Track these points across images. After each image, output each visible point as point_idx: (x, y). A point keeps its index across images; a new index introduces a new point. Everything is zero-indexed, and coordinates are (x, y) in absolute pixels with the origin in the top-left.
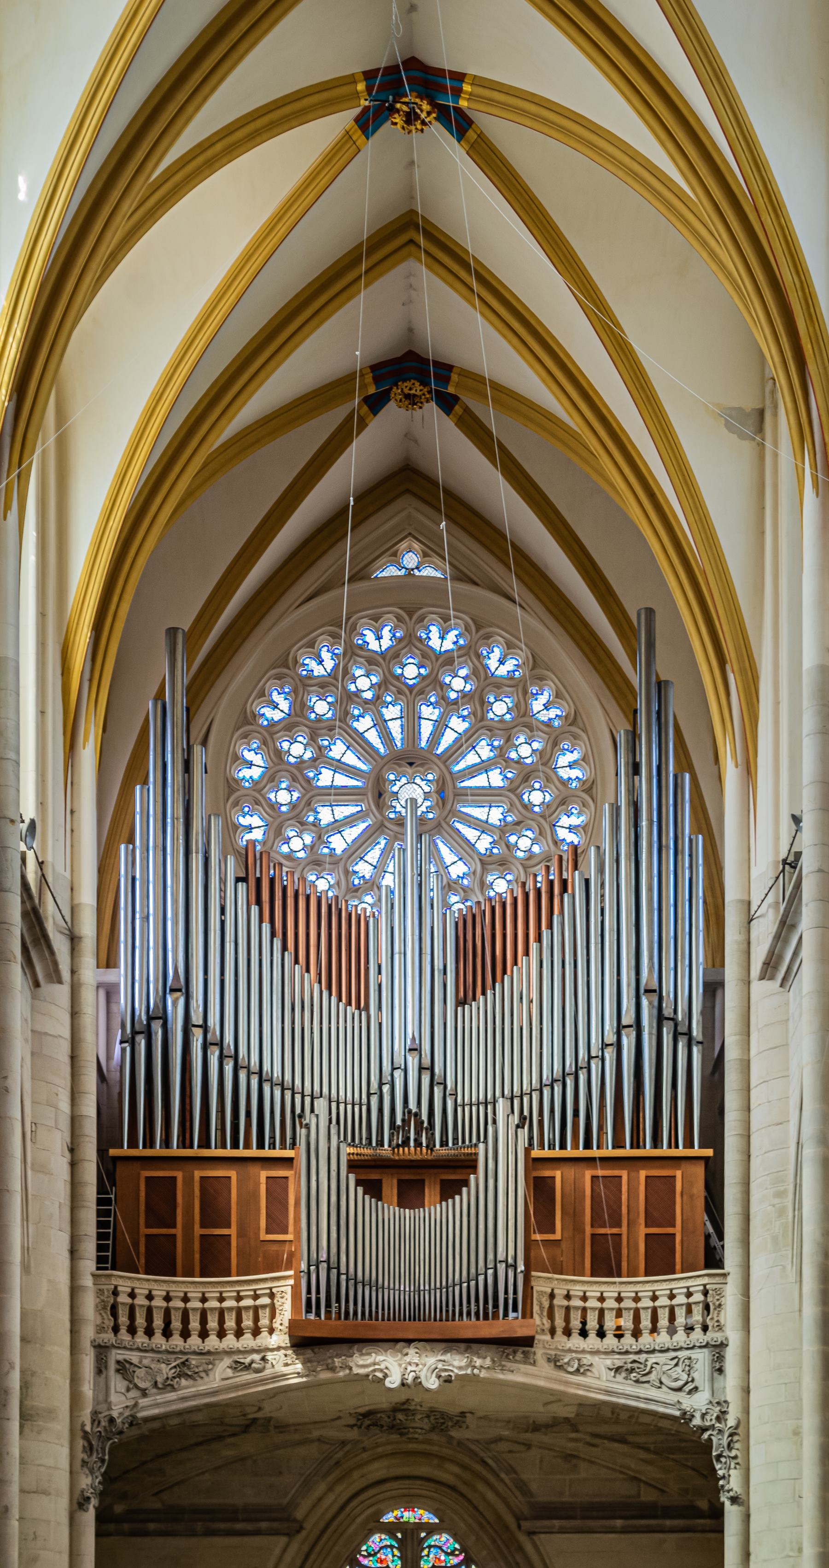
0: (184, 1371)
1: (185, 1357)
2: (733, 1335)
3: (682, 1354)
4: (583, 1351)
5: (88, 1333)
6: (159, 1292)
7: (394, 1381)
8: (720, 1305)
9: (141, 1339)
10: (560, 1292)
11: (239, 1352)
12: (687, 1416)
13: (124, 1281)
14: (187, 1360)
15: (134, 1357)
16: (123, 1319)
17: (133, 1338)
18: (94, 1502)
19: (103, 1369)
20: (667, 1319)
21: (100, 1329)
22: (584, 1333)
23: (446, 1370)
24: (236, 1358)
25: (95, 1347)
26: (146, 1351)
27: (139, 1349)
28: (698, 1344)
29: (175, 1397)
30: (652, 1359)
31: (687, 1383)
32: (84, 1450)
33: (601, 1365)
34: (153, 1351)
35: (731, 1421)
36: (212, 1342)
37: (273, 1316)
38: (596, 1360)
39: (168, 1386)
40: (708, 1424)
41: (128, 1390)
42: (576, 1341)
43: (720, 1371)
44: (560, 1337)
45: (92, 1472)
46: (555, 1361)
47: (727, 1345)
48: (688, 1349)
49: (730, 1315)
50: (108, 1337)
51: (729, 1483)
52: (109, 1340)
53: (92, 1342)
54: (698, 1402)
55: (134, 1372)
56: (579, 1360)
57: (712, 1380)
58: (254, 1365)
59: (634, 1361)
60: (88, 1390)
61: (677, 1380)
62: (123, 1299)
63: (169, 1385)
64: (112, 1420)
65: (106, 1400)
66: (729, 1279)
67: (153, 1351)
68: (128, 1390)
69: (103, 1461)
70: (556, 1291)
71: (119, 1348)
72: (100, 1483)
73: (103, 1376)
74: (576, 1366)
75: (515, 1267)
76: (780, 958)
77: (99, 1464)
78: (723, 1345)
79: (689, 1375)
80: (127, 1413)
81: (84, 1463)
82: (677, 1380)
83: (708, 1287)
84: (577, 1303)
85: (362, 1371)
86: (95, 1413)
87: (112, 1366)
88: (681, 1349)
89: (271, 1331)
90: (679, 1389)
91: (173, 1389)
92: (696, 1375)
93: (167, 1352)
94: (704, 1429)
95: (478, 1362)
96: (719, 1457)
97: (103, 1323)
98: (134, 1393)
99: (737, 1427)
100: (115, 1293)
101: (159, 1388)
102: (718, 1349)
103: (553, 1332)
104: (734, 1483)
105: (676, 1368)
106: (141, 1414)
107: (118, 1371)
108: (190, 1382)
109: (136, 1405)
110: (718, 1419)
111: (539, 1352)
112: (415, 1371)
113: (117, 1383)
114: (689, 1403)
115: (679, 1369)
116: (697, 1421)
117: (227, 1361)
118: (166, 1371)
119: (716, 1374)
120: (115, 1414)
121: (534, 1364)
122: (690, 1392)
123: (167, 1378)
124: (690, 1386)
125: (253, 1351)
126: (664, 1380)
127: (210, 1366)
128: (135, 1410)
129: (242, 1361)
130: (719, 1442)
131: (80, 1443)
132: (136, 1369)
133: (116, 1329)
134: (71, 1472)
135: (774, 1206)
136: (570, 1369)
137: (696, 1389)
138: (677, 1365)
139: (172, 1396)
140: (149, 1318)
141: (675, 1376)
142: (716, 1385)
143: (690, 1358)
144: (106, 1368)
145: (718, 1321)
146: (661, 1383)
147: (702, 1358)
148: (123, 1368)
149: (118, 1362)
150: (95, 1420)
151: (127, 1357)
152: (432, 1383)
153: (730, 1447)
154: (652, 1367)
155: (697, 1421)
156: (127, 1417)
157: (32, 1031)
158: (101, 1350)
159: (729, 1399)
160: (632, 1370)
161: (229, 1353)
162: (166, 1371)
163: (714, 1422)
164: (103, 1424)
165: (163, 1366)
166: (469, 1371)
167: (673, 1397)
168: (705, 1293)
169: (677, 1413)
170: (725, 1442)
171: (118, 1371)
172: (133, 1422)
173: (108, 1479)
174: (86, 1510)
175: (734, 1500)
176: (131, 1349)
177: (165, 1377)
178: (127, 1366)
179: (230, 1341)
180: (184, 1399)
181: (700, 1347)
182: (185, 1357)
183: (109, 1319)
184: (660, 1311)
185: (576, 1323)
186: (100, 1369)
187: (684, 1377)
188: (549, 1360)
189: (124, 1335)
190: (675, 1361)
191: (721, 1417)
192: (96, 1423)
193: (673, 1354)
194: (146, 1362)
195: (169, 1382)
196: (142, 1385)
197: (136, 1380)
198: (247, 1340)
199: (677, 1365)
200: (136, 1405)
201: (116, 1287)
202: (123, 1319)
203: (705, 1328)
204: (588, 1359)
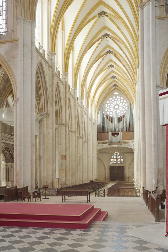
0: (102, 146)
5: (97, 144)
6: (101, 141)
7: (114, 147)
13: (99, 141)
33: (127, 145)
36: (104, 144)
39: (102, 147)
46: (124, 145)
50: (98, 144)
54: (132, 147)
60: (97, 148)
102: (133, 144)
111: (123, 144)
113: (99, 147)
130: (134, 150)
148: (99, 146)
152: (116, 147)
158: (98, 145)
162: (101, 146)
172: (100, 149)
186: (98, 146)
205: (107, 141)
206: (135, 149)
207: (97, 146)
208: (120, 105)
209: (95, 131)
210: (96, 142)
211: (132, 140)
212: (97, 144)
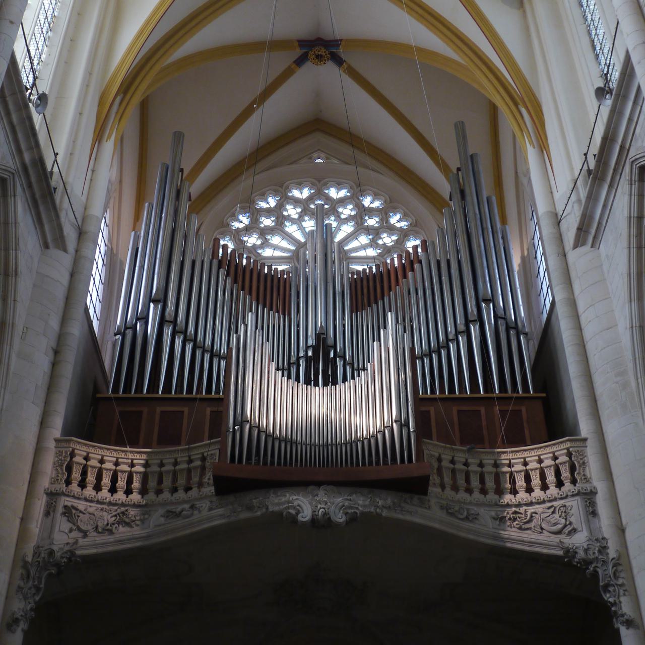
1: (123, 509)
2: (599, 484)
3: (554, 503)
4: (470, 503)
5: (45, 483)
8: (584, 463)
9: (89, 491)
10: (446, 457)
11: (172, 503)
12: (570, 553)
13: (81, 448)
14: (127, 511)
15: (81, 505)
16: (76, 475)
17: (82, 490)
18: (23, 625)
19: (52, 514)
20: (538, 479)
21: (54, 481)
22: (469, 491)
23: (351, 508)
24: (169, 508)
25: (47, 494)
26: (91, 501)
27: (86, 500)
28: (570, 494)
29: (112, 540)
30: (531, 510)
31: (565, 526)
32: (22, 578)
34: (98, 502)
35: (612, 553)
37: (203, 474)
38: (482, 511)
40: (592, 557)
41: (71, 531)
42: (462, 495)
43: (594, 513)
44: (449, 492)
45: (25, 598)
47: (596, 493)
48: (561, 499)
49: (593, 468)
51: (621, 609)
52: (60, 489)
53: (45, 490)
55: (78, 516)
56: (468, 510)
57: (588, 522)
58: (184, 512)
59: (515, 512)
60: (35, 528)
61: (555, 524)
62: (79, 459)
63: (108, 530)
64: (51, 553)
65: (50, 536)
66: (589, 443)
67: (98, 502)
68: (71, 531)
69: (38, 589)
70: (443, 456)
71: (68, 496)
72: (31, 609)
73: (50, 518)
74: (465, 513)
75: (407, 425)
76: (591, 218)
77: (33, 591)
78: (593, 493)
79: (566, 519)
80: (67, 548)
81: (20, 588)
82: (555, 524)
83: (571, 449)
84: (459, 466)
85: (276, 509)
86: (38, 547)
87: (60, 509)
88: (555, 499)
89: (200, 485)
90: (559, 532)
91: (111, 532)
92: (573, 519)
93: (110, 504)
94: (588, 563)
95: (380, 503)
96: (606, 586)
97: (58, 476)
98: (76, 534)
99: (619, 558)
100: (72, 455)
101: (99, 533)
103: (443, 487)
104: (626, 607)
105: (554, 515)
106: (78, 552)
107: (64, 514)
108: (127, 529)
109: (76, 542)
110: (599, 551)
112: (324, 508)
113: (63, 524)
114: (569, 541)
115: (556, 516)
116: (581, 554)
117: (161, 511)
118: (108, 517)
119: (590, 517)
120: (55, 548)
121: (429, 508)
122: (570, 533)
123: (108, 524)
124: (569, 528)
125: (185, 502)
126: (544, 526)
127: (146, 516)
128: (74, 547)
129: (174, 510)
130: (605, 573)
131: (20, 571)
132: (81, 514)
133: (68, 482)
134: (7, 598)
135: (617, 383)
136: (461, 517)
137: (574, 531)
138: (553, 512)
139: (111, 538)
140: (99, 478)
141: (553, 521)
142: (592, 526)
143: (565, 506)
144: (54, 511)
145: (584, 475)
146: (542, 529)
147: (575, 505)
148: (69, 512)
149: (65, 507)
150: (36, 553)
151: (75, 505)
153: (616, 576)
154: (532, 517)
155: (581, 554)
156: (66, 553)
157: (37, 272)
158: (52, 496)
159: (606, 536)
160: (515, 519)
161: (164, 504)
163: (597, 554)
164: (43, 555)
165: (105, 514)
166: (372, 510)
167: (555, 539)
168: (569, 454)
169: (561, 553)
170: (610, 571)
171: (64, 514)
173: (39, 608)
174: (14, 632)
175: (629, 623)
176: (79, 499)
177: (106, 523)
178: (74, 511)
179: (166, 495)
180: (120, 542)
181: (572, 496)
182: (123, 509)
183: (63, 474)
184: (532, 474)
185: (461, 482)
186: (49, 512)
187: (564, 521)
188: (442, 508)
189: (75, 488)
190: (552, 509)
191: (603, 549)
192: (37, 554)
193: (549, 504)
194: (91, 510)
195: (109, 527)
196: (84, 527)
197: (79, 523)
198: (181, 494)
199: (553, 512)
200: (76, 542)
201: (73, 450)
202: (76, 475)
203: (574, 482)
204: (474, 509)
205: (209, 449)
206: (622, 563)
207: (40, 504)
208: (356, 250)
209: (55, 323)
210: (39, 450)
211: (560, 448)
212: (45, 483)
